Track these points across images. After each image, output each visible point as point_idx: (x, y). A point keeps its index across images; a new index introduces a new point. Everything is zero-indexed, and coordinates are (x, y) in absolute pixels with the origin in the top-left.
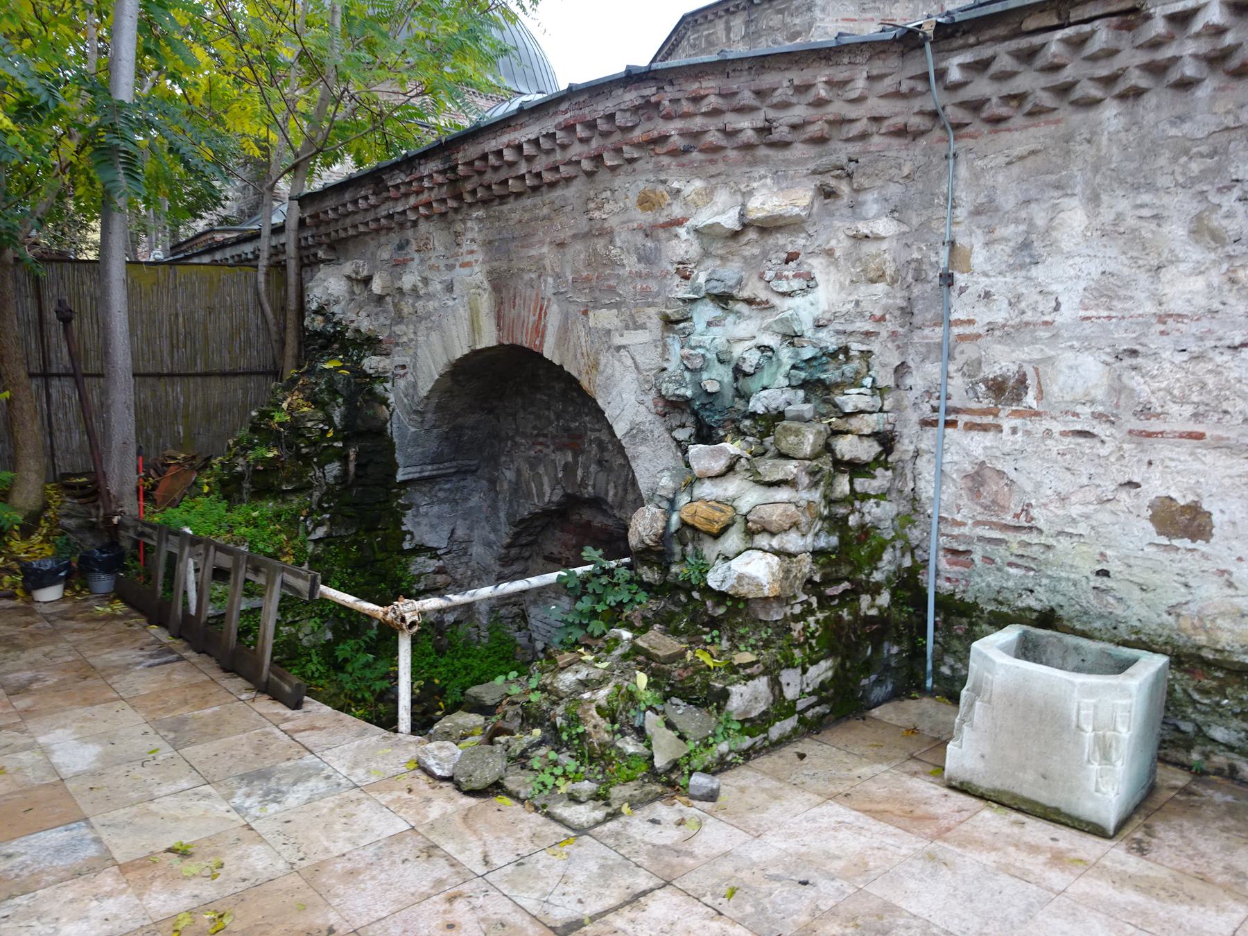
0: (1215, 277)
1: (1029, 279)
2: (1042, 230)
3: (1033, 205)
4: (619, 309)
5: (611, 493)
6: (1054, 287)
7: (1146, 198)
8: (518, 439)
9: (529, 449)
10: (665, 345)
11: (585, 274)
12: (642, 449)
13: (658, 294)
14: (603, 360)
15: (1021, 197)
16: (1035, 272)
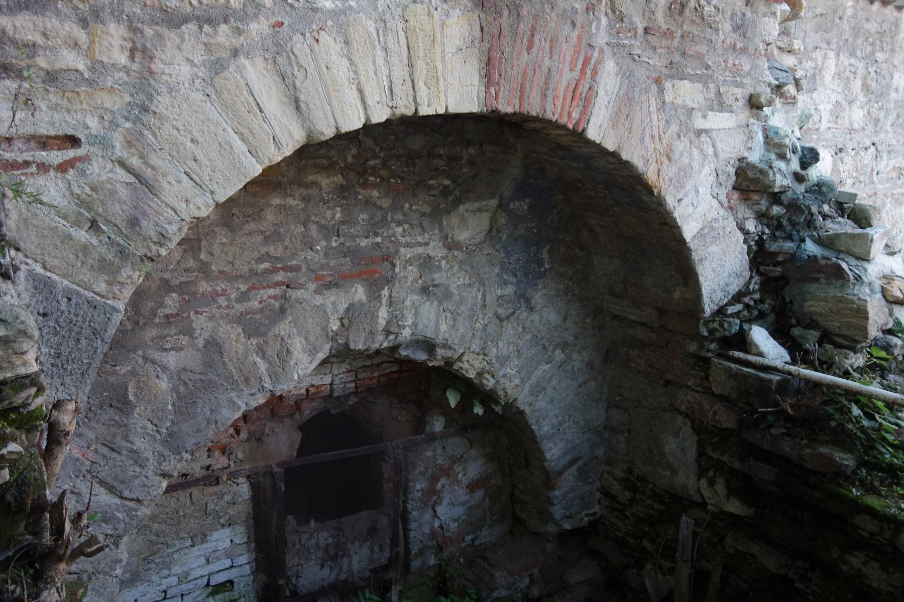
0: (866, 112)
1: (812, 98)
2: (819, 68)
3: (818, 50)
4: (705, 84)
5: (444, 327)
6: (821, 107)
7: (853, 61)
8: (204, 287)
9: (243, 297)
10: (750, 132)
11: (664, 27)
12: (713, 248)
13: (749, 74)
14: (680, 146)
15: (815, 44)
16: (815, 95)
